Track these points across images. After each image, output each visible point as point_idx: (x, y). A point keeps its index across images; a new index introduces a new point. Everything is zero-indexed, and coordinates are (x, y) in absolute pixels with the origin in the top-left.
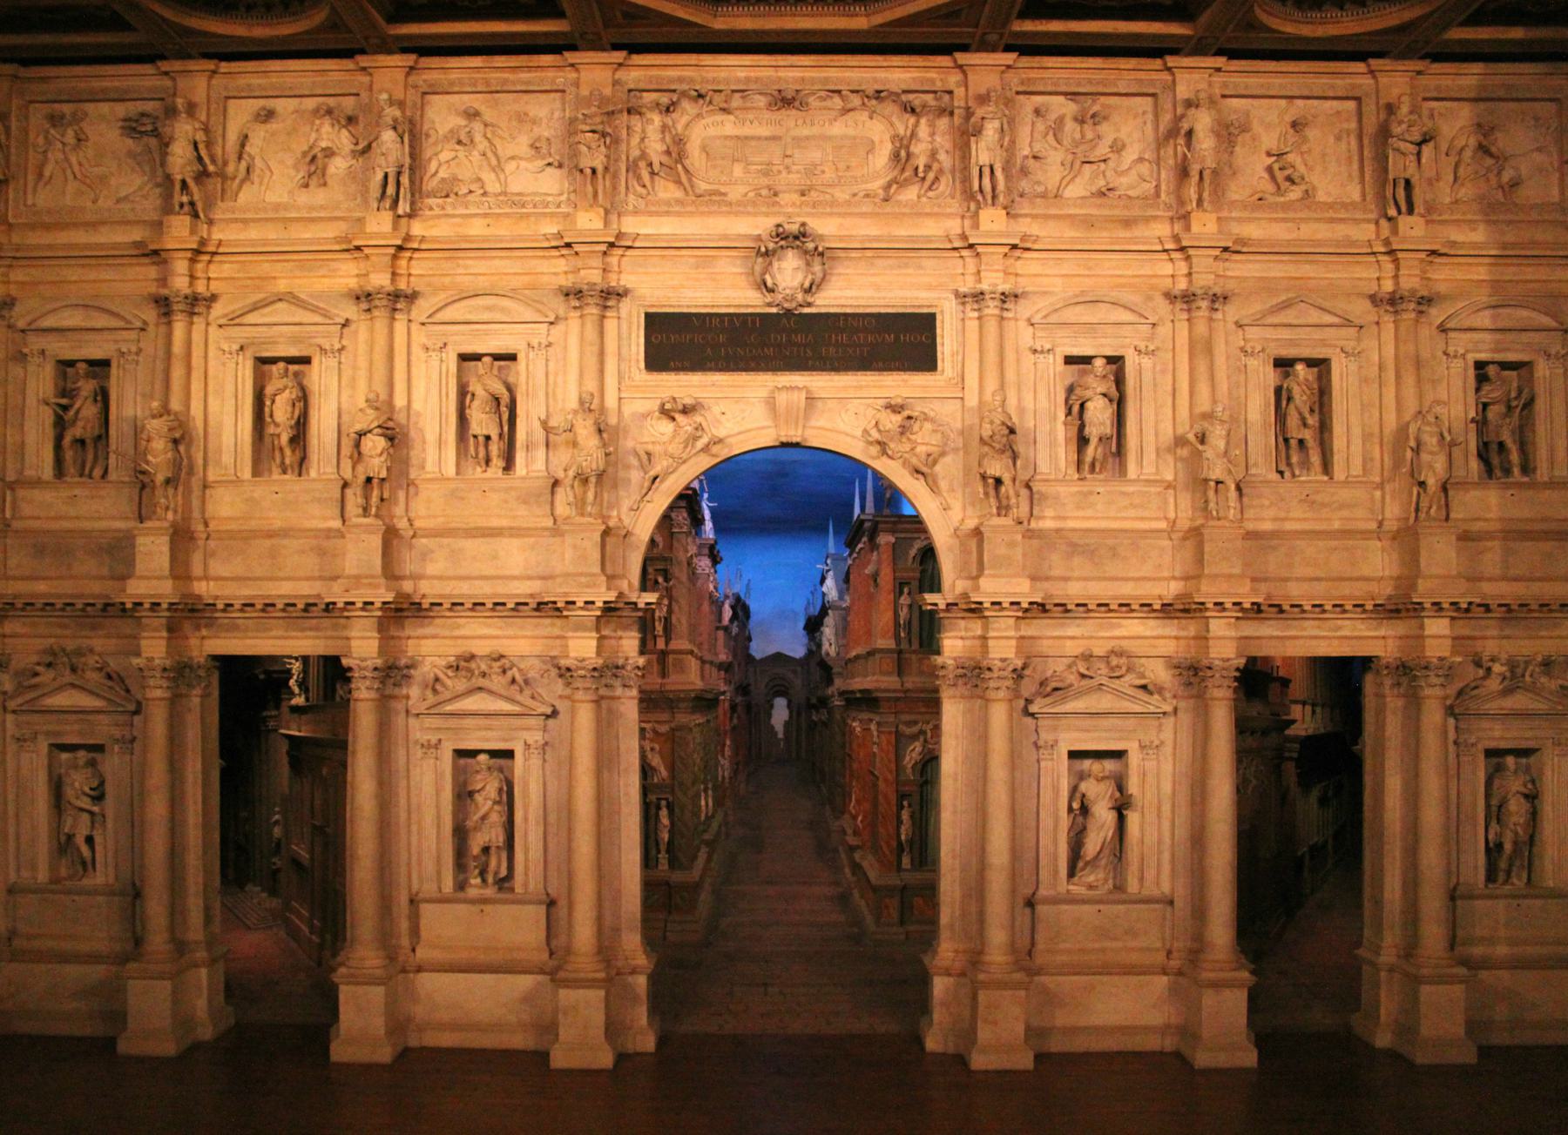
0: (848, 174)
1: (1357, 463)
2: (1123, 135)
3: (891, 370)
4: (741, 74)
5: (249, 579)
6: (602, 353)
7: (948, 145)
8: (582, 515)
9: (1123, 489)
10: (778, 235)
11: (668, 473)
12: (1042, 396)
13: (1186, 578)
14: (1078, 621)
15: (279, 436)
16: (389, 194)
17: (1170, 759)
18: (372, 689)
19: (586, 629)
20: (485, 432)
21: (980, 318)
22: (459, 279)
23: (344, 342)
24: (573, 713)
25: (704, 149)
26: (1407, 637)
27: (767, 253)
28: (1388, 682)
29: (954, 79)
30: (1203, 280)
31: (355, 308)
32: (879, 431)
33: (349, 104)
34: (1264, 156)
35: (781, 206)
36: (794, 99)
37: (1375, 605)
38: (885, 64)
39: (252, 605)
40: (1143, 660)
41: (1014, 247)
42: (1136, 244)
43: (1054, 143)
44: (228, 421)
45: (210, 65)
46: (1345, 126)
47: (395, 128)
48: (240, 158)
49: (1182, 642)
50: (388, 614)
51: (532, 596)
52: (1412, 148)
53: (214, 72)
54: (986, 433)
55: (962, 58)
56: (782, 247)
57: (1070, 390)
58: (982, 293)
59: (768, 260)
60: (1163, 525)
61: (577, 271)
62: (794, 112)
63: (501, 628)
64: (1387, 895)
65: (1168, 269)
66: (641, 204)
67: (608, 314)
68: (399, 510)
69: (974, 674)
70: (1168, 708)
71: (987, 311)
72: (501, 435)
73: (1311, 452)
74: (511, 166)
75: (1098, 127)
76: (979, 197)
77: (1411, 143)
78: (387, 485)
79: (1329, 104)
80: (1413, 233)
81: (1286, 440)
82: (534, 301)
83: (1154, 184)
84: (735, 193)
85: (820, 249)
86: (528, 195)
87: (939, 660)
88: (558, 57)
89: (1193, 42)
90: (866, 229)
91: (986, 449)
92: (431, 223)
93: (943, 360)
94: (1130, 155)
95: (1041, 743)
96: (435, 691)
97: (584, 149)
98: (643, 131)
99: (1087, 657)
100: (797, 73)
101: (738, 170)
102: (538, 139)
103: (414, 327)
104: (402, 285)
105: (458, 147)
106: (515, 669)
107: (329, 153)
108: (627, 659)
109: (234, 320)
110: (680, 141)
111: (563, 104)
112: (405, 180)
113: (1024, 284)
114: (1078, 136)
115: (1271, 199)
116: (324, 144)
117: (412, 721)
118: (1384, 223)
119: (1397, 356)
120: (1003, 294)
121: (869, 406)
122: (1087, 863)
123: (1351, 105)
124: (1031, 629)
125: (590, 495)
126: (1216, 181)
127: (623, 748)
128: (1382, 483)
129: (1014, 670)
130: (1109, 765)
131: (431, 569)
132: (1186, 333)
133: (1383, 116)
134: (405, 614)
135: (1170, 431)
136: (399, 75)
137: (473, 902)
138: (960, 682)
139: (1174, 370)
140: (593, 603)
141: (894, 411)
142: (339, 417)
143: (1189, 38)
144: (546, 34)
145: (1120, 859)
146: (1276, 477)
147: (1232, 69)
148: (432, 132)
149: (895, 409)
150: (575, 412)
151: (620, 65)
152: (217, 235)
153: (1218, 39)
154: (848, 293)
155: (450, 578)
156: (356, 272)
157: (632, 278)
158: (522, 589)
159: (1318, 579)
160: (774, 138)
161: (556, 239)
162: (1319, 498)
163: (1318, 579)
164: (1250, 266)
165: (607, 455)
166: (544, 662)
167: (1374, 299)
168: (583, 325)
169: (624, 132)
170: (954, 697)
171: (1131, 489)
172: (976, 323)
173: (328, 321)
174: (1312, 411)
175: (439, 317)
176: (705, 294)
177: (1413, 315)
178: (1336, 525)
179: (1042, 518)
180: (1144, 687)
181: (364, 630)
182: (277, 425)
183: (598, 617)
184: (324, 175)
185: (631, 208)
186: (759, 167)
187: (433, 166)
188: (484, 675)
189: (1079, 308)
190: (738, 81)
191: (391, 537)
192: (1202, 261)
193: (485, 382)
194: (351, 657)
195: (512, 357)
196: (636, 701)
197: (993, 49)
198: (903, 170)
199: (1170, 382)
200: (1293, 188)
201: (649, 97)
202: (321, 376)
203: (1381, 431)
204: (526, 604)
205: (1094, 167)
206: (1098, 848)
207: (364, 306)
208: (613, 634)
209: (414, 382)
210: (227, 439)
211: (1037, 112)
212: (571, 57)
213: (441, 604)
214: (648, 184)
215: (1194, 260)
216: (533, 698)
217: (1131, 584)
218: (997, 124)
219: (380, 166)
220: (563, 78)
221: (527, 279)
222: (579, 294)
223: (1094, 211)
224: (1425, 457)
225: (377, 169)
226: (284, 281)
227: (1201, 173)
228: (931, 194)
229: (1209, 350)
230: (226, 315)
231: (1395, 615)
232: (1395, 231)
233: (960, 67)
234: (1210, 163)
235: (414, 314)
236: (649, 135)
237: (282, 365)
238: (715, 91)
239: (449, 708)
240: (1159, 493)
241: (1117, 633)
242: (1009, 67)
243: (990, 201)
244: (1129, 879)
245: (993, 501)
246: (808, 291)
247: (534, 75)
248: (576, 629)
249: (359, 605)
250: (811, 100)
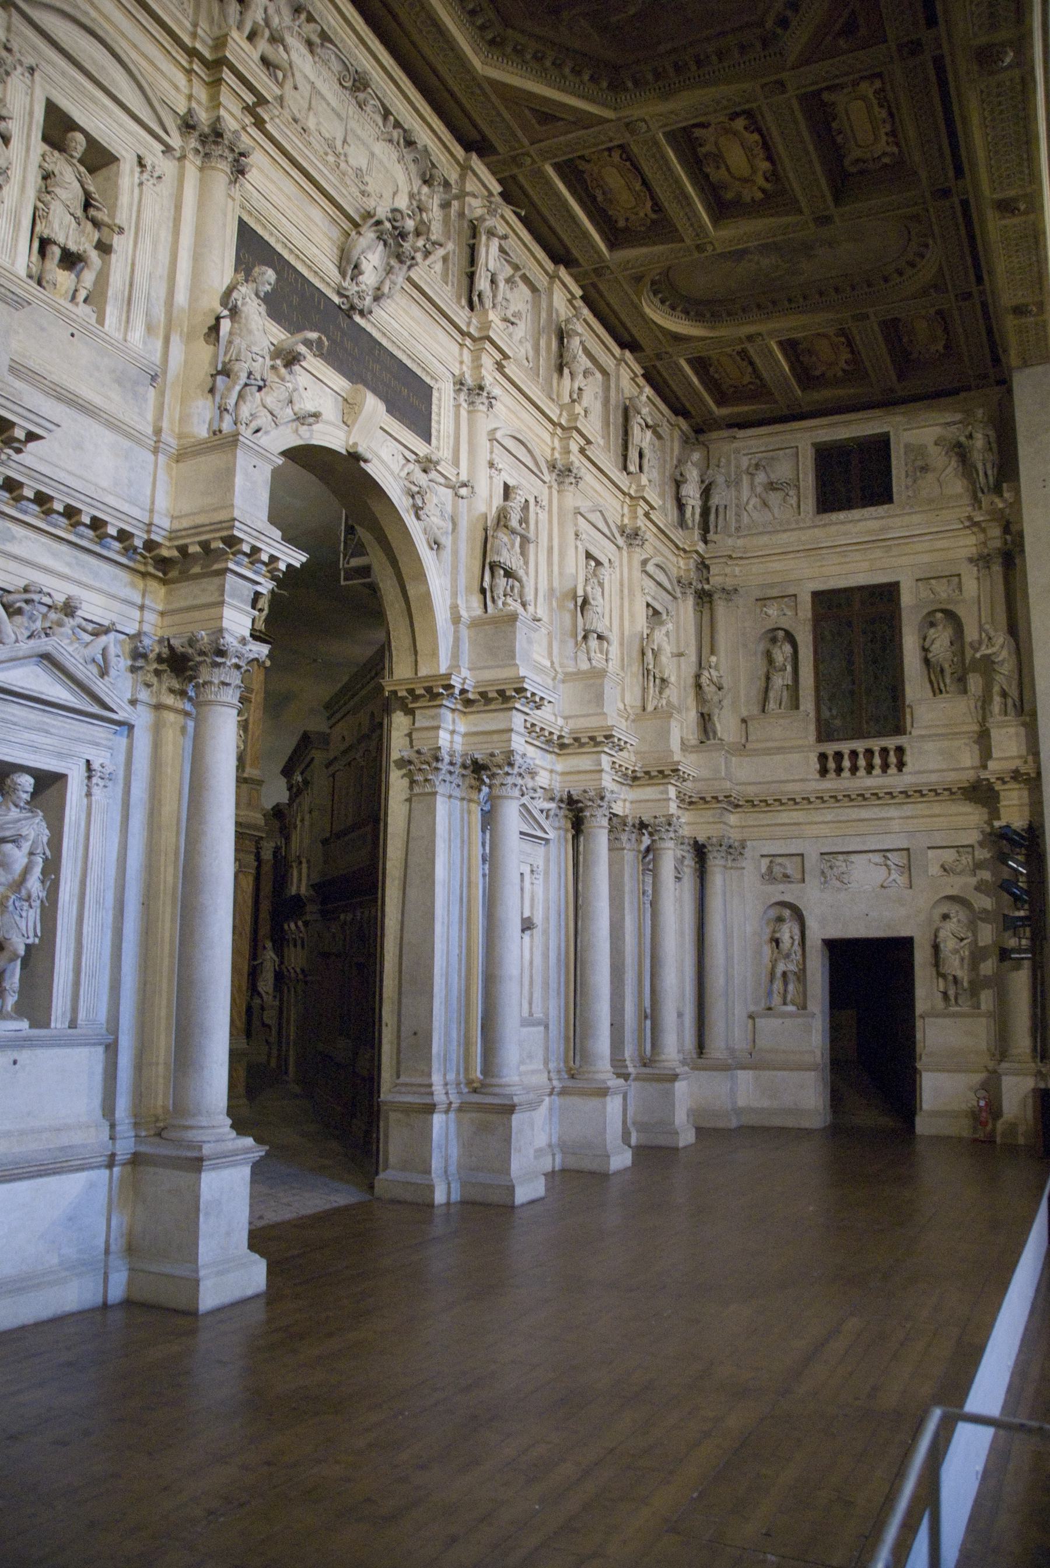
20: (73, 247)
26: (640, 801)
49: (554, 775)
55: (476, 162)
63: (69, 564)
93: (438, 439)
138: (448, 778)
170: (444, 795)
180: (542, 811)
197: (494, 173)
224: (664, 659)
248: (232, 596)
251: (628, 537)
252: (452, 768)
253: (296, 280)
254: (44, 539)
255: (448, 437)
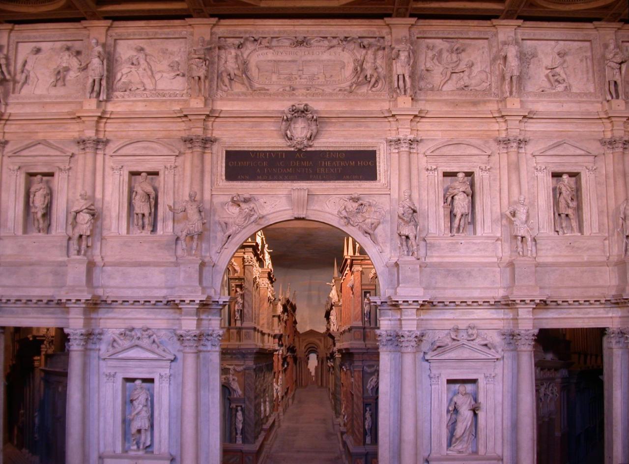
0: (333, 79)
1: (596, 225)
2: (472, 59)
3: (353, 180)
4: (276, 29)
5: (19, 287)
6: (202, 172)
7: (384, 65)
8: (191, 255)
9: (474, 241)
10: (293, 111)
11: (236, 233)
12: (431, 192)
13: (508, 288)
14: (453, 311)
15: (37, 213)
16: (95, 90)
17: (501, 385)
18: (79, 345)
19: (191, 315)
20: (142, 212)
21: (398, 153)
22: (130, 133)
23: (72, 165)
24: (184, 360)
25: (257, 66)
27: (287, 120)
28: (614, 341)
29: (384, 31)
30: (514, 133)
31: (77, 148)
32: (346, 211)
33: (78, 45)
34: (544, 70)
35: (297, 96)
36: (303, 42)
37: (606, 301)
38: (349, 24)
39: (20, 300)
40: (486, 331)
41: (416, 116)
42: (479, 114)
43: (437, 63)
44: (11, 205)
45: (10, 26)
46: (585, 54)
47: (99, 57)
48: (22, 72)
50: (89, 306)
51: (164, 297)
52: (618, 66)
53: (11, 30)
54: (401, 211)
55: (388, 20)
56: (295, 117)
57: (446, 190)
58: (399, 140)
59: (288, 123)
60: (495, 260)
61: (190, 129)
62: (303, 48)
64: (615, 454)
65: (496, 127)
66: (225, 95)
67: (206, 151)
68: (97, 252)
69: (396, 339)
70: (498, 356)
71: (402, 149)
72: (150, 214)
73: (572, 221)
74: (158, 76)
75: (459, 55)
76: (398, 91)
77: (617, 63)
78: (90, 239)
79: (576, 43)
80: (620, 108)
81: (559, 215)
82: (168, 144)
83: (489, 83)
84: (273, 89)
85: (315, 117)
86: (166, 90)
87: (378, 332)
88: (183, 21)
89: (505, 12)
90: (339, 107)
91: (400, 221)
92: (117, 105)
94: (476, 70)
95: (432, 375)
96: (113, 346)
97: (195, 67)
98: (226, 58)
99: (457, 330)
100: (305, 29)
101: (274, 78)
102: (172, 63)
103: (107, 157)
104: (101, 136)
105: (133, 66)
106: (155, 336)
107: (67, 69)
108: (213, 331)
109: (16, 154)
110: (245, 63)
111: (186, 44)
112: (104, 83)
113: (421, 135)
114: (449, 60)
115: (549, 91)
116: (64, 65)
117: (102, 363)
118: (605, 103)
119: (614, 171)
120: (410, 140)
121: (341, 199)
122: (457, 439)
123: (587, 44)
124: (424, 316)
125: (194, 246)
126: (519, 81)
127: (211, 378)
128: (609, 237)
129: (416, 337)
130: (469, 387)
131: (112, 283)
132: (506, 159)
133: (602, 50)
134: (99, 306)
135: (499, 211)
136: (103, 30)
137: (132, 458)
138: (390, 343)
139: (500, 179)
140: (194, 301)
141: (354, 201)
142: (67, 203)
143: (504, 10)
144: (176, 10)
145: (476, 437)
146: (552, 233)
147: (526, 26)
148: (119, 59)
149: (355, 200)
150: (187, 202)
151: (214, 25)
152: (9, 111)
153: (516, 11)
154: (330, 140)
155: (123, 288)
156: (78, 129)
157: (219, 132)
158: (161, 294)
159: (576, 287)
160: (294, 61)
161: (179, 113)
162: (576, 245)
163: (576, 287)
164: (539, 125)
165: (203, 224)
166: (171, 332)
167: (603, 142)
168: (193, 157)
169: (216, 59)
171: (479, 241)
172: (397, 155)
173: (64, 155)
174: (572, 199)
175: (120, 152)
176: (256, 141)
177: (621, 150)
178: (586, 259)
179: (432, 257)
180: (486, 345)
181: (77, 314)
182: (36, 208)
183: (198, 308)
184: (64, 80)
185: (219, 97)
186: (285, 76)
187: (119, 76)
188: (139, 338)
189: (450, 147)
190: (275, 32)
191: (91, 266)
192: (514, 123)
193: (142, 186)
194: (68, 328)
195: (156, 174)
196: (218, 353)
197: (404, 16)
198: (359, 77)
199: (498, 186)
200: (560, 85)
201: (230, 41)
202: (59, 183)
203: (608, 209)
204: (161, 302)
205: (458, 75)
206: (463, 431)
207: (82, 147)
208: (207, 318)
209: (106, 186)
210: (11, 214)
211: (428, 47)
212: (189, 21)
213: (116, 301)
214: (228, 84)
215: (509, 122)
216: (164, 351)
217: (479, 290)
218: (406, 53)
219: (91, 76)
220: (184, 32)
221: (163, 132)
222: (191, 141)
223: (457, 97)
225: (90, 77)
226: (42, 134)
227: (511, 77)
228: (374, 89)
229: (518, 169)
230: (12, 151)
231: (617, 306)
232: (611, 108)
233: (388, 25)
234: (516, 73)
235: (107, 151)
236: (229, 60)
237: (39, 177)
238: (263, 38)
239: (120, 356)
240: (493, 243)
241: (471, 317)
242: (412, 25)
243: (403, 93)
244: (480, 447)
245: (405, 248)
246: (310, 139)
247: (171, 30)
249: (74, 301)
250: (312, 42)
251: (610, 143)
252: (389, 338)
253: (265, 155)
254: (137, 310)
255: (385, 172)
